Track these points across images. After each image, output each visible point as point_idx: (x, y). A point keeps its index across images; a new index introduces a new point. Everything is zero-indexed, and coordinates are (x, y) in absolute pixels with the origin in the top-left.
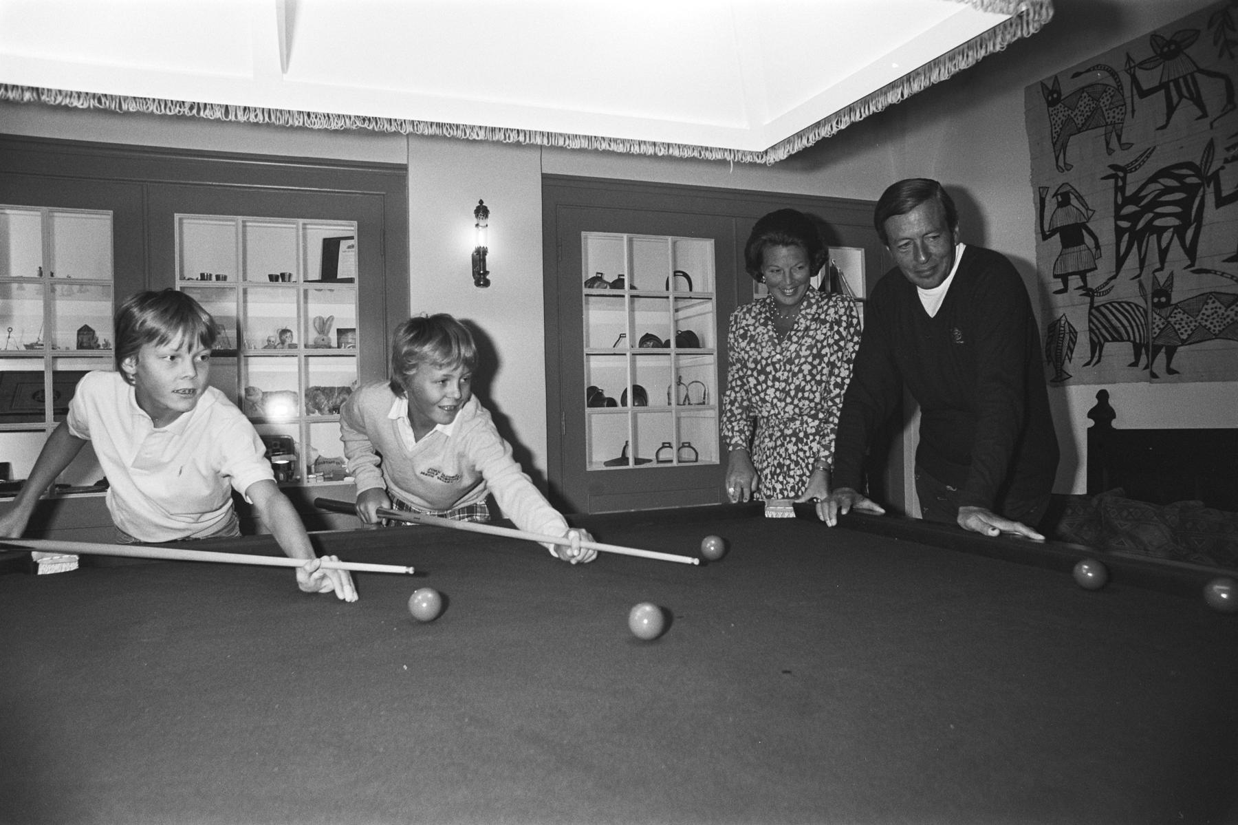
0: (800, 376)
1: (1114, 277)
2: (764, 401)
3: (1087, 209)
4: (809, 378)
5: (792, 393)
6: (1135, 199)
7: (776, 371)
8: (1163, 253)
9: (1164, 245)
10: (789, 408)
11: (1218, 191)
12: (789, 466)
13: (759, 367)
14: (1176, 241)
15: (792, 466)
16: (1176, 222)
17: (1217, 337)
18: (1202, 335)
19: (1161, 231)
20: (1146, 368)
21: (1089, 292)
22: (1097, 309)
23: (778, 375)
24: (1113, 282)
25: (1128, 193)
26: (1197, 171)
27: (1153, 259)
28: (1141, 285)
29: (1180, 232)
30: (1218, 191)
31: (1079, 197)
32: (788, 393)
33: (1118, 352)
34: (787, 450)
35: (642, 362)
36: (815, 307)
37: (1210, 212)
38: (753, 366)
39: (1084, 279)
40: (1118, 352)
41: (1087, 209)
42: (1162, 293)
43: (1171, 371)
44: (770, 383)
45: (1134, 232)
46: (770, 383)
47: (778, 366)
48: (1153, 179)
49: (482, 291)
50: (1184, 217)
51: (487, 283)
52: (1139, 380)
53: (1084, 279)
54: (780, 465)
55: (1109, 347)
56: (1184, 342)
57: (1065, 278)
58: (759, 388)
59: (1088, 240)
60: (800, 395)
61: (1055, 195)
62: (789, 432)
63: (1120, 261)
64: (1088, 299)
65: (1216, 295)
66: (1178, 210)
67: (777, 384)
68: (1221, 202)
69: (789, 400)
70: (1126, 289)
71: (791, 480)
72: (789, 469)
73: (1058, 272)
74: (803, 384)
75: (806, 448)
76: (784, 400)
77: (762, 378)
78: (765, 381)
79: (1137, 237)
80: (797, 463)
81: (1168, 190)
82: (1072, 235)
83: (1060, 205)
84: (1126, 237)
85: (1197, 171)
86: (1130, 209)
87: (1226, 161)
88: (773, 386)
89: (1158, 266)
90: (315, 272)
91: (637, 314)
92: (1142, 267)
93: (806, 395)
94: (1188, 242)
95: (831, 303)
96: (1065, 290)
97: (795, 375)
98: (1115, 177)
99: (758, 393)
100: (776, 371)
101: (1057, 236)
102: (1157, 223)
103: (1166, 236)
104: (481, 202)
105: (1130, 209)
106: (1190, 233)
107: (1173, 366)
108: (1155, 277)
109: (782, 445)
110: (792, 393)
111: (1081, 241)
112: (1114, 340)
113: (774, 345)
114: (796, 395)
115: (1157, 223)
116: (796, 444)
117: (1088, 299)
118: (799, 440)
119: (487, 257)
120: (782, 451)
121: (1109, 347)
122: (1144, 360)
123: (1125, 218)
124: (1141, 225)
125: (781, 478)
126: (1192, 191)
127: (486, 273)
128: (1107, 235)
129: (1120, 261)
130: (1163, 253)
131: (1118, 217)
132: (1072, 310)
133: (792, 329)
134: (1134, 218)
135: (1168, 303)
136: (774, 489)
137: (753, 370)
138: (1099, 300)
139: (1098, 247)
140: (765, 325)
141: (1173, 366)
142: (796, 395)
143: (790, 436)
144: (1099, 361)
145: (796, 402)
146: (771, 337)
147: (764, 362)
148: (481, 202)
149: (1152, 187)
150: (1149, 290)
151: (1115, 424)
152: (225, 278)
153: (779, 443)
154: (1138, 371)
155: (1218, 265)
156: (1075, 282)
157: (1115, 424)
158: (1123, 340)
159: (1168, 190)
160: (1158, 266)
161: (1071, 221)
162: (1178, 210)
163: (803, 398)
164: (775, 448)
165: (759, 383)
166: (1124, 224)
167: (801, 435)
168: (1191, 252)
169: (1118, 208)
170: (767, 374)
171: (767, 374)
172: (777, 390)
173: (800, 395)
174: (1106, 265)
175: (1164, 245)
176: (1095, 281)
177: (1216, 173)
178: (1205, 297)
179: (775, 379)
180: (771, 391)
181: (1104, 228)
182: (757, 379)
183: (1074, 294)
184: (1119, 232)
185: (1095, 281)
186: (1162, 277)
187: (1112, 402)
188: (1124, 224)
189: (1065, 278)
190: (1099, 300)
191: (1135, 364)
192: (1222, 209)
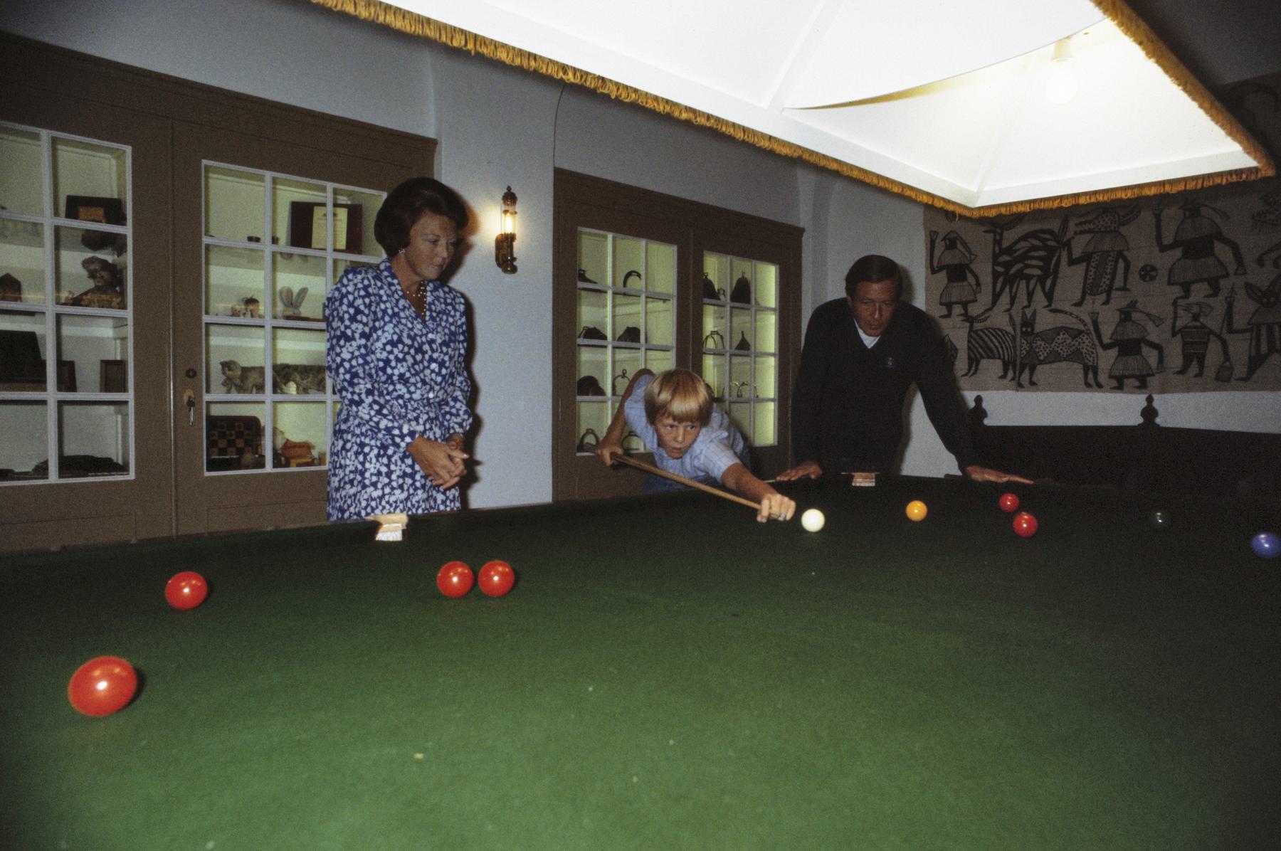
1: (990, 309)
6: (1009, 251)
7: (433, 351)
8: (1030, 295)
9: (1031, 288)
11: (1070, 254)
14: (1039, 288)
16: (1037, 272)
17: (1065, 360)
18: (1055, 358)
19: (1028, 278)
20: (1013, 379)
21: (970, 319)
22: (976, 332)
24: (990, 313)
25: (1005, 244)
26: (1056, 238)
28: (1011, 318)
29: (1041, 279)
30: (1070, 254)
33: (992, 367)
35: (735, 360)
37: (1065, 269)
39: (966, 309)
40: (992, 367)
42: (1028, 323)
43: (1032, 383)
44: (426, 364)
45: (1007, 277)
48: (1024, 238)
49: (509, 278)
50: (1045, 269)
51: (514, 270)
52: (1005, 388)
53: (966, 309)
55: (984, 362)
56: (1041, 362)
57: (949, 306)
59: (971, 279)
63: (996, 297)
64: (968, 324)
66: (1041, 264)
68: (1072, 262)
70: (999, 319)
73: (944, 300)
79: (1010, 281)
81: (1034, 248)
82: (957, 273)
84: (1001, 280)
85: (1056, 238)
86: (1006, 258)
87: (1076, 233)
89: (1026, 303)
90: (283, 232)
91: (735, 319)
94: (1047, 287)
96: (948, 316)
98: (994, 232)
99: (417, 374)
100: (433, 351)
101: (944, 273)
102: (1028, 271)
103: (1033, 282)
104: (509, 189)
105: (1006, 258)
106: (1049, 282)
107: (1034, 379)
108: (1024, 313)
111: (965, 279)
112: (989, 357)
115: (1028, 271)
117: (968, 324)
119: (515, 244)
121: (984, 362)
122: (1010, 374)
124: (1013, 271)
126: (1051, 251)
127: (514, 259)
128: (986, 279)
129: (996, 297)
130: (1030, 295)
131: (995, 263)
132: (956, 332)
134: (1007, 265)
137: (410, 347)
138: (977, 326)
139: (978, 284)
141: (1034, 379)
144: (975, 372)
148: (509, 189)
149: (1023, 244)
150: (1018, 320)
151: (987, 422)
152: (258, 240)
154: (1006, 382)
155: (1067, 307)
156: (957, 310)
157: (987, 422)
158: (994, 358)
159: (1034, 248)
160: (1026, 303)
161: (956, 262)
162: (1041, 264)
165: (416, 362)
166: (1000, 269)
168: (1049, 296)
169: (995, 257)
171: (424, 353)
174: (985, 298)
175: (1031, 288)
176: (975, 310)
177: (1069, 241)
178: (1058, 330)
181: (984, 269)
182: (414, 357)
183: (956, 318)
184: (996, 275)
185: (975, 310)
186: (1029, 312)
187: (985, 405)
188: (1000, 269)
189: (949, 306)
190: (977, 326)
191: (1004, 377)
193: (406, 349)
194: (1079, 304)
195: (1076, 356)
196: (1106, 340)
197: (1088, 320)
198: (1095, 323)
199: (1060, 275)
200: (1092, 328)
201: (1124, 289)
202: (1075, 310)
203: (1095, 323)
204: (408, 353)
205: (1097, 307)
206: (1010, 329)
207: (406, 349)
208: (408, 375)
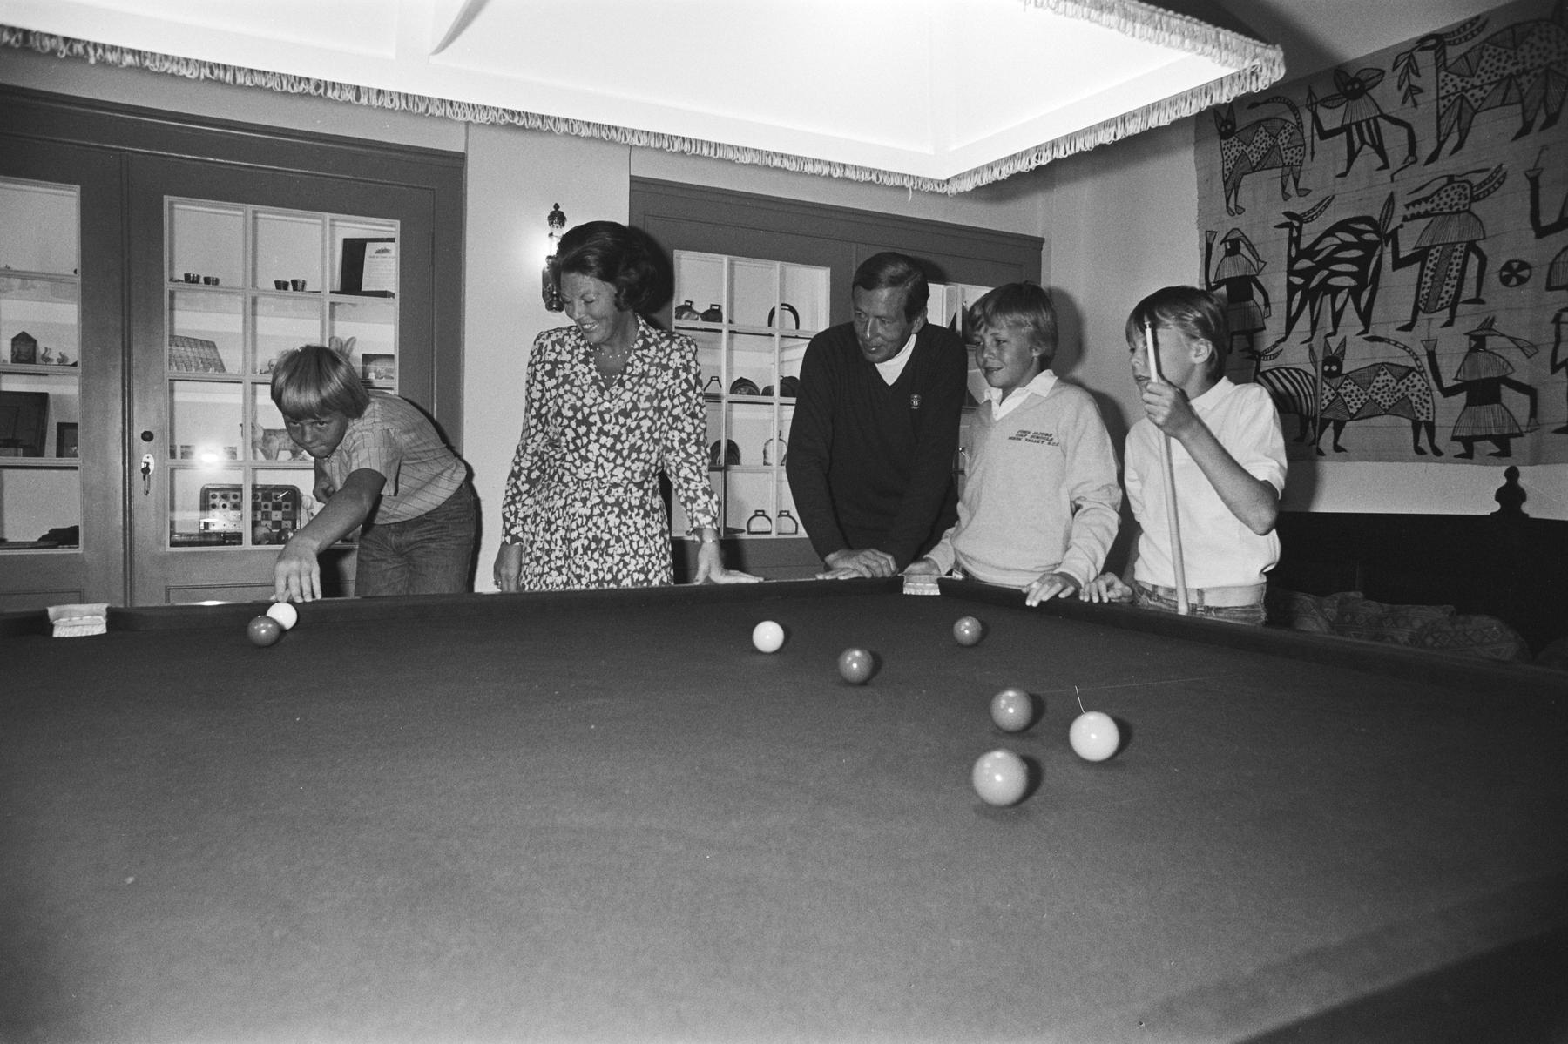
0: (638, 433)
1: (1283, 340)
2: (585, 459)
3: (1258, 260)
4: (647, 436)
5: (625, 453)
6: (1310, 253)
8: (1337, 316)
9: (1338, 306)
10: (619, 471)
11: (1396, 251)
12: (607, 542)
13: (579, 416)
14: (1350, 303)
15: (612, 542)
16: (1352, 282)
23: (606, 428)
25: (1304, 244)
27: (1326, 320)
28: (1311, 350)
29: (1355, 293)
30: (1396, 251)
31: (1250, 246)
32: (619, 453)
34: (606, 521)
36: (653, 348)
38: (571, 414)
41: (1258, 260)
42: (1335, 359)
46: (593, 437)
47: (607, 417)
48: (1330, 232)
54: (597, 539)
56: (1353, 417)
58: (578, 442)
59: (1258, 297)
60: (634, 456)
61: (1224, 241)
62: (612, 500)
63: (1291, 322)
65: (1388, 366)
66: (1354, 268)
67: (603, 439)
68: (1399, 263)
69: (619, 461)
71: (609, 559)
72: (607, 545)
74: (640, 442)
75: (630, 522)
76: (614, 460)
77: (582, 429)
78: (587, 434)
79: (1311, 296)
80: (618, 540)
81: (1345, 246)
83: (1229, 253)
84: (1298, 296)
86: (1304, 264)
87: (1405, 219)
88: (597, 441)
89: (1330, 330)
92: (1313, 332)
93: (642, 456)
95: (675, 346)
97: (630, 431)
98: (1289, 225)
99: (577, 449)
102: (1334, 281)
105: (1304, 264)
109: (601, 515)
110: (625, 453)
113: (602, 391)
114: (629, 456)
115: (1334, 281)
116: (618, 516)
118: (623, 512)
120: (601, 522)
123: (1299, 273)
124: (1314, 283)
125: (596, 556)
126: (1369, 248)
128: (1278, 295)
129: (1291, 322)
131: (1291, 272)
133: (624, 373)
134: (1308, 274)
135: (1338, 373)
136: (587, 568)
137: (570, 419)
139: (1267, 304)
140: (585, 362)
142: (629, 456)
143: (612, 505)
145: (628, 463)
146: (595, 380)
147: (586, 411)
149: (1328, 241)
150: (1320, 357)
153: (597, 511)
159: (1345, 246)
160: (1330, 330)
162: (1354, 268)
163: (638, 459)
164: (590, 517)
165: (578, 436)
166: (1298, 281)
167: (625, 506)
168: (1366, 317)
169: (1291, 262)
170: (590, 426)
172: (603, 446)
173: (634, 456)
175: (1338, 306)
177: (1395, 231)
178: (1377, 368)
179: (601, 432)
180: (594, 447)
182: (575, 431)
184: (1292, 289)
186: (1334, 343)
188: (1298, 281)
192: (1399, 271)
193: (566, 422)
194: (1408, 328)
195: (1401, 406)
196: (1448, 382)
197: (1421, 351)
198: (1432, 356)
199: (1382, 283)
200: (1425, 361)
201: (1477, 300)
202: (1404, 337)
203: (1432, 356)
204: (569, 426)
205: (1436, 331)
206: (1310, 369)
207: (566, 422)
208: (640, 442)
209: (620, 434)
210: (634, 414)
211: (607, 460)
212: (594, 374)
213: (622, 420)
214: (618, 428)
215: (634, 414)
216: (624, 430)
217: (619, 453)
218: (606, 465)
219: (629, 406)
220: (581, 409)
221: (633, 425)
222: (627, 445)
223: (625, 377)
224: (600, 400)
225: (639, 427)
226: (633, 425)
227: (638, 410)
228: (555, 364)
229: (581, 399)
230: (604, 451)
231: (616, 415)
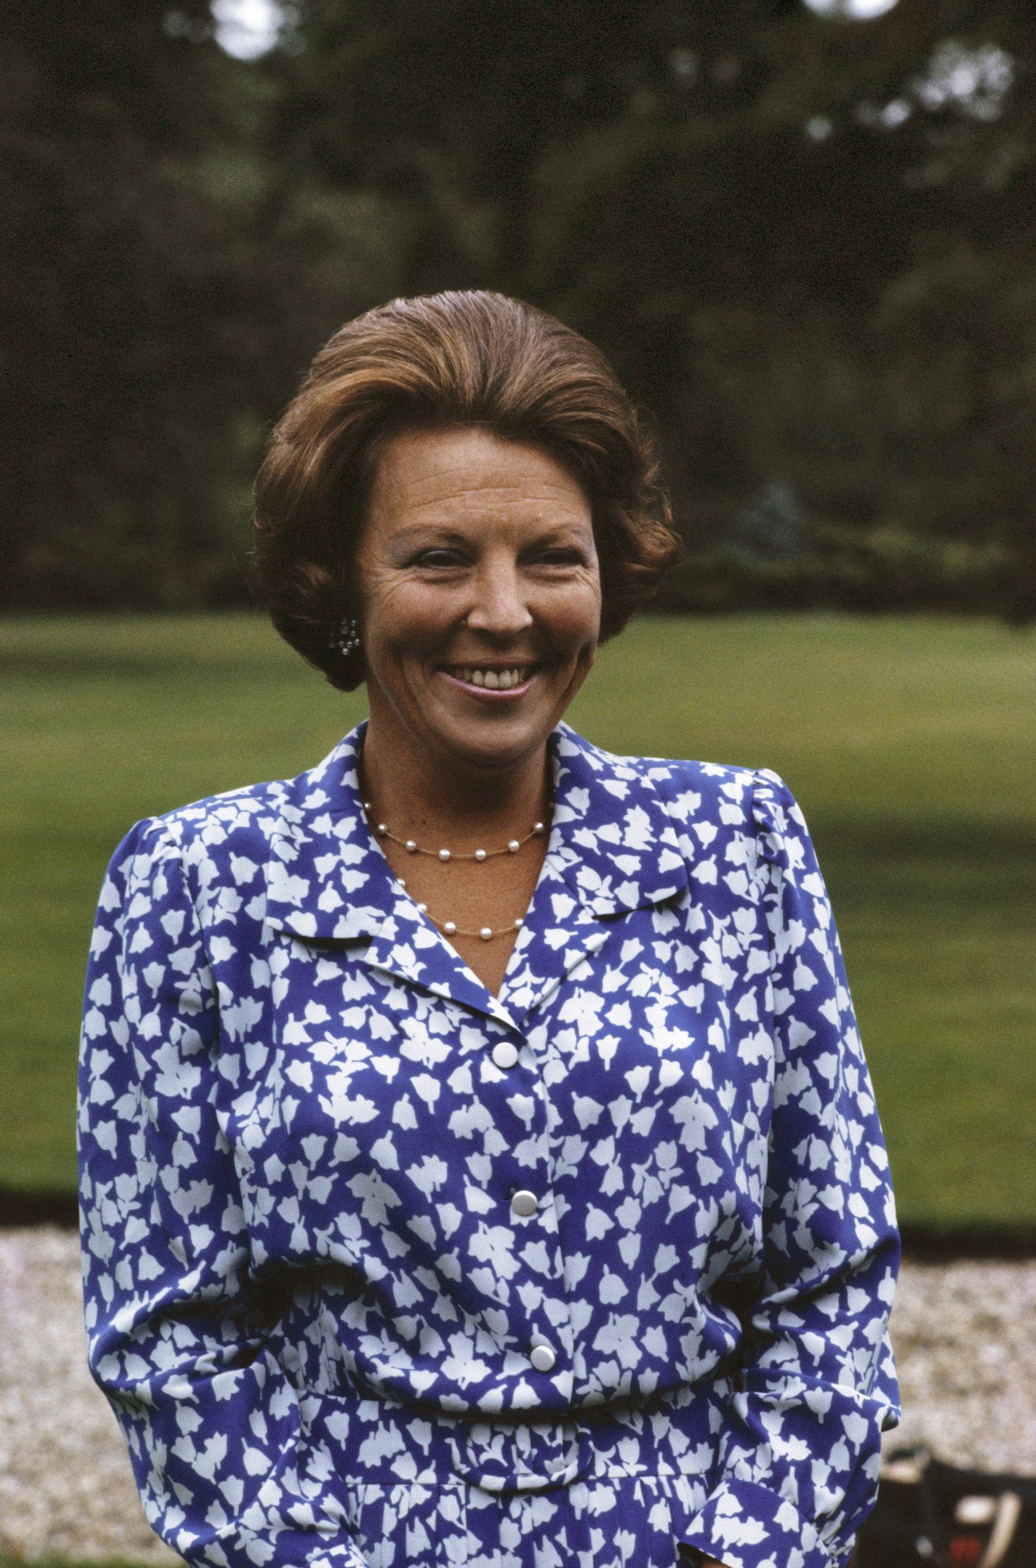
0: (666, 1154)
5: (630, 1249)
10: (618, 1337)
32: (604, 1253)
38: (364, 1111)
60: (666, 1258)
62: (600, 1500)
69: (612, 1288)
74: (682, 1198)
76: (588, 1289)
97: (633, 1149)
110: (630, 1249)
114: (646, 1261)
142: (646, 1261)
143: (610, 1522)
147: (427, 1088)
173: (666, 1258)
209: (591, 1171)
210: (638, 1078)
211: (555, 1288)
212: (425, 938)
213: (586, 1109)
214: (575, 1147)
215: (638, 1078)
216: (605, 1152)
217: (604, 1253)
218: (555, 1310)
219: (608, 1048)
220: (403, 1085)
221: (643, 1122)
222: (629, 1214)
223: (556, 938)
224: (472, 1040)
225: (667, 1128)
226: (643, 1122)
227: (651, 1058)
228: (245, 934)
229: (391, 1047)
230: (536, 1255)
231: (561, 1094)
